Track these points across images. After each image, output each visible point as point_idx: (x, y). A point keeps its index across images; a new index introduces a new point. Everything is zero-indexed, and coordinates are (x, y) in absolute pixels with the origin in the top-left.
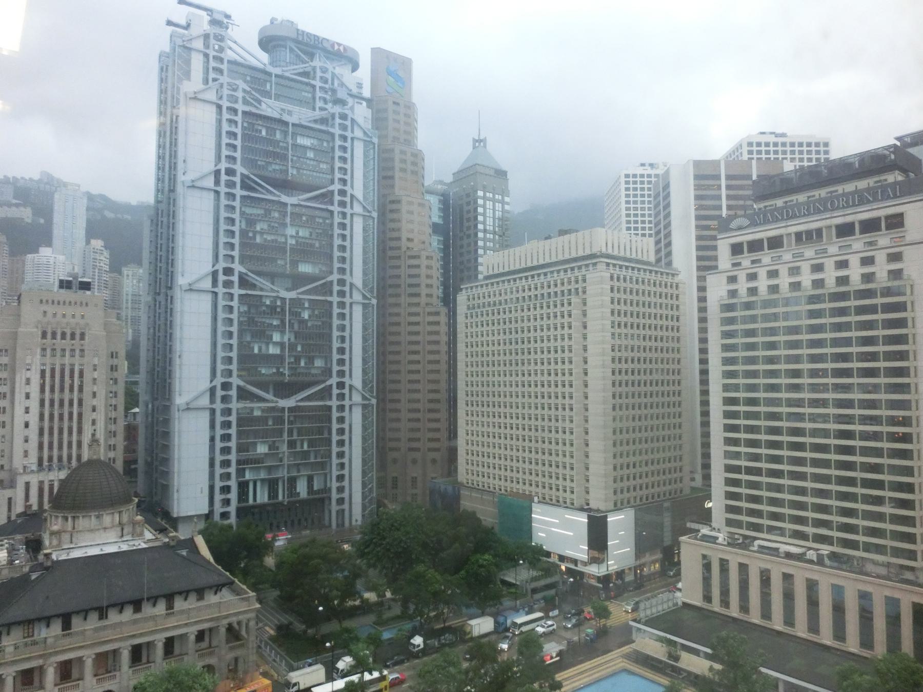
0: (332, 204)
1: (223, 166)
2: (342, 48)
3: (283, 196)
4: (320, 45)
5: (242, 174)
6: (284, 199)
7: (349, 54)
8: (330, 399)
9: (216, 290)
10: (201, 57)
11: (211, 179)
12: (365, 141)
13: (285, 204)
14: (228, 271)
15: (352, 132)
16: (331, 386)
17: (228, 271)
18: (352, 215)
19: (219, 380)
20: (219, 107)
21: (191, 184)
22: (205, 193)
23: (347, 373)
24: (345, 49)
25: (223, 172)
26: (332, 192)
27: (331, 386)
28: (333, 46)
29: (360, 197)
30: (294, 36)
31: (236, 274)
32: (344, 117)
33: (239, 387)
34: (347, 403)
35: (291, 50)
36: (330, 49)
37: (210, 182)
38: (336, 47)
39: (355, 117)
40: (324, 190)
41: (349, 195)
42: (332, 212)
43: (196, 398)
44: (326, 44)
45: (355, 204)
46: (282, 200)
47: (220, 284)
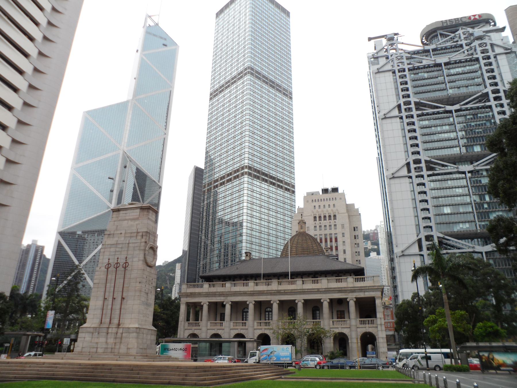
0: (489, 101)
1: (402, 101)
2: (477, 17)
4: (460, 22)
6: (449, 108)
7: (484, 17)
9: (410, 174)
11: (397, 109)
12: (506, 53)
13: (450, 112)
14: (417, 162)
15: (493, 51)
17: (417, 162)
20: (394, 72)
22: (394, 120)
24: (480, 16)
25: (402, 104)
26: (487, 94)
28: (470, 18)
30: (440, 25)
31: (423, 161)
36: (468, 21)
37: (396, 112)
39: (494, 42)
41: (502, 91)
42: (490, 107)
44: (464, 20)
47: (413, 170)
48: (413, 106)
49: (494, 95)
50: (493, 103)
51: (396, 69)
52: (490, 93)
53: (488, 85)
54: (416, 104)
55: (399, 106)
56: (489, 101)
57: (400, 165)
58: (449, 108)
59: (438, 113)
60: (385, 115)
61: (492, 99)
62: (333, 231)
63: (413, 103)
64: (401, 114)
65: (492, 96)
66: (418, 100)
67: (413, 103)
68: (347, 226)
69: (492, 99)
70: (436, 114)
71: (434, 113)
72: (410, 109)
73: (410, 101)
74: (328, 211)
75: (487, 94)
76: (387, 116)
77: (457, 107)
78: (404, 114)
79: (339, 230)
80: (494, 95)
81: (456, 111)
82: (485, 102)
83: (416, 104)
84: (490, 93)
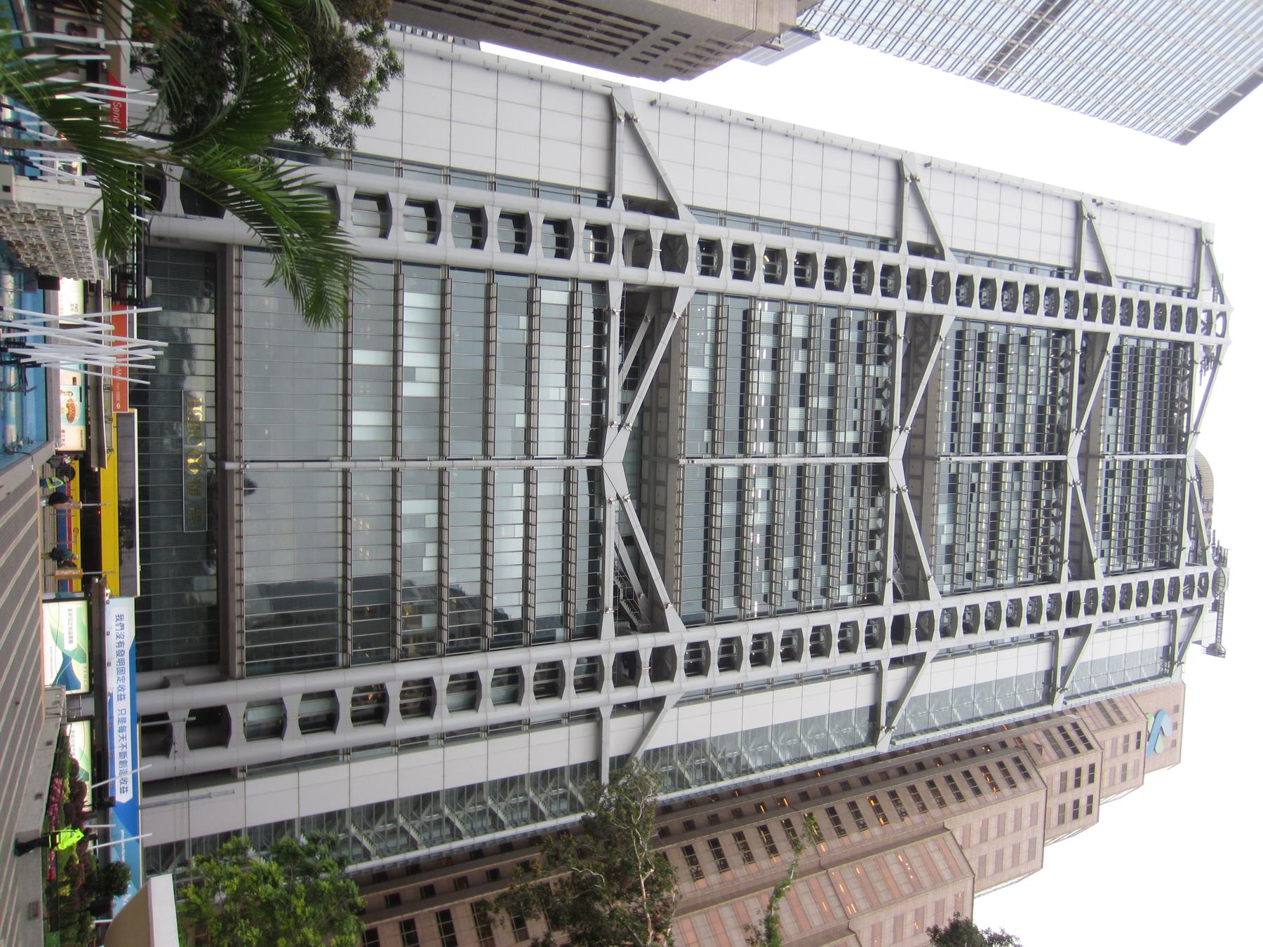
1: (693, 230)
3: (625, 434)
5: (673, 291)
6: (617, 443)
11: (647, 191)
13: (596, 449)
18: (592, 715)
21: (620, 111)
26: (659, 625)
29: (656, 740)
37: (633, 182)
40: (664, 596)
41: (661, 689)
42: (592, 632)
45: (634, 721)
46: (611, 433)
48: (655, 275)
49: (645, 658)
50: (609, 645)
52: (660, 639)
53: (697, 634)
54: (666, 295)
55: (666, 208)
56: (620, 632)
58: (617, 443)
59: (600, 394)
60: (629, 119)
61: (627, 643)
63: (671, 279)
64: (618, 203)
65: (644, 644)
66: (678, 308)
67: (671, 279)
69: (627, 643)
70: (597, 382)
71: (600, 371)
72: (640, 258)
73: (681, 269)
75: (659, 625)
76: (621, 128)
77: (616, 482)
78: (620, 219)
80: (645, 658)
81: (595, 476)
82: (620, 615)
83: (666, 295)
84: (660, 639)
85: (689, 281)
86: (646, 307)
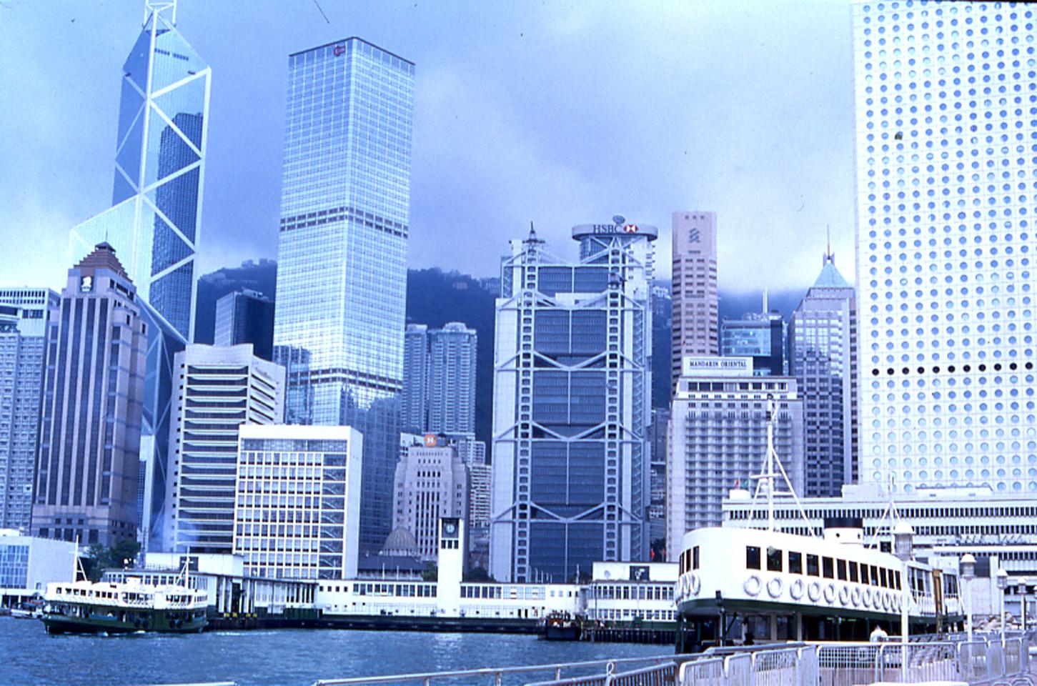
2: (633, 229)
5: (535, 356)
8: (603, 519)
10: (520, 270)
16: (603, 509)
17: (525, 426)
18: (622, 373)
19: (519, 502)
23: (617, 499)
27: (603, 509)
30: (592, 231)
32: (614, 296)
33: (532, 508)
34: (616, 522)
35: (592, 240)
38: (628, 229)
39: (626, 294)
43: (504, 514)
51: (523, 308)
57: (508, 429)
62: (436, 489)
68: (450, 483)
74: (430, 467)
78: (521, 369)
79: (442, 489)
85: (532, 352)
86: (538, 362)
